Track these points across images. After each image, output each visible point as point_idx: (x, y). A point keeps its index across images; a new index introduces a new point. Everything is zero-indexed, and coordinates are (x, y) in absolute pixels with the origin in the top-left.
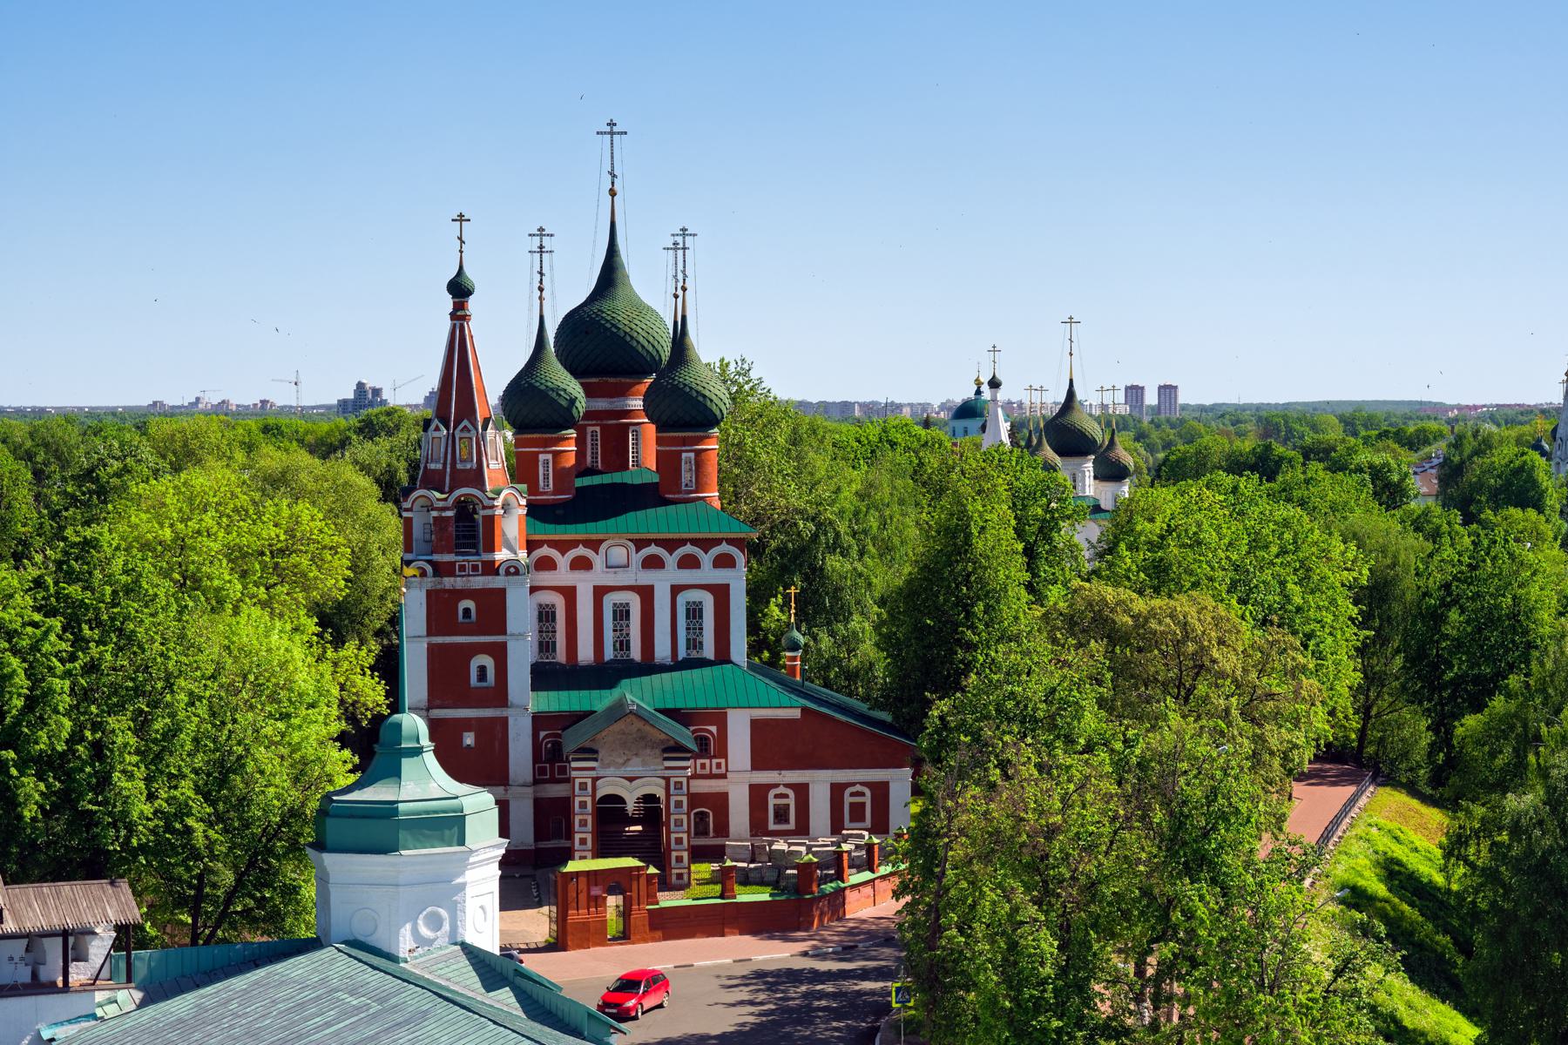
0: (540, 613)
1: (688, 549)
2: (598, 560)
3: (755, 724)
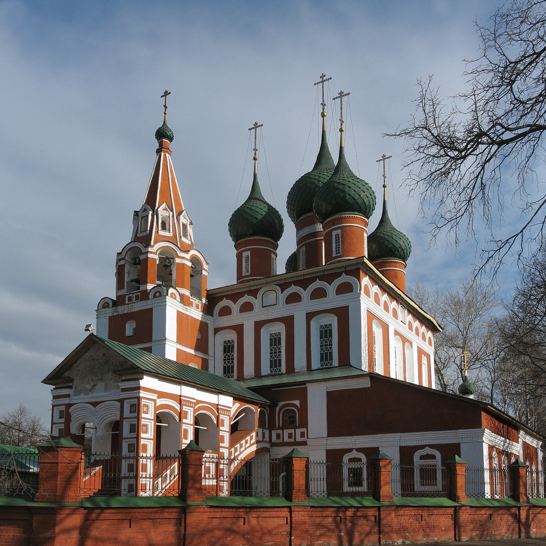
0: (225, 347)
1: (318, 284)
2: (256, 302)
3: (330, 395)
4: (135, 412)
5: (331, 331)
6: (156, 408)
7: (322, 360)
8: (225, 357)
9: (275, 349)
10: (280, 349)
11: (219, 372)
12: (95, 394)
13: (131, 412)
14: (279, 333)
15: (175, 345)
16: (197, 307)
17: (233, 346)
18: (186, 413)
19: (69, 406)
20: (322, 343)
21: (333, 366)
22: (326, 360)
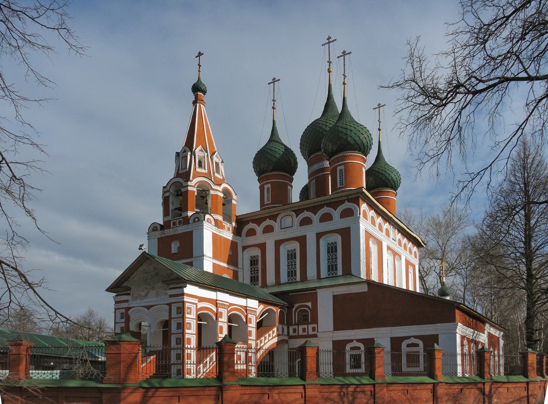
0: (251, 261)
1: (326, 210)
2: (276, 225)
3: (336, 299)
4: (181, 313)
5: (336, 247)
6: (197, 310)
7: (329, 271)
8: (251, 269)
9: (292, 263)
10: (295, 262)
11: (247, 281)
12: (148, 300)
13: (177, 313)
14: (295, 250)
15: (211, 260)
16: (229, 229)
17: (258, 260)
18: (221, 313)
19: (128, 309)
20: (329, 257)
21: (338, 275)
22: (332, 270)
